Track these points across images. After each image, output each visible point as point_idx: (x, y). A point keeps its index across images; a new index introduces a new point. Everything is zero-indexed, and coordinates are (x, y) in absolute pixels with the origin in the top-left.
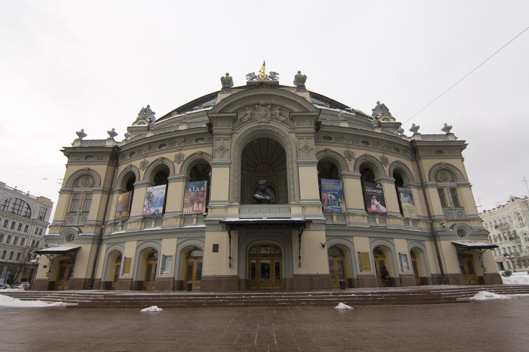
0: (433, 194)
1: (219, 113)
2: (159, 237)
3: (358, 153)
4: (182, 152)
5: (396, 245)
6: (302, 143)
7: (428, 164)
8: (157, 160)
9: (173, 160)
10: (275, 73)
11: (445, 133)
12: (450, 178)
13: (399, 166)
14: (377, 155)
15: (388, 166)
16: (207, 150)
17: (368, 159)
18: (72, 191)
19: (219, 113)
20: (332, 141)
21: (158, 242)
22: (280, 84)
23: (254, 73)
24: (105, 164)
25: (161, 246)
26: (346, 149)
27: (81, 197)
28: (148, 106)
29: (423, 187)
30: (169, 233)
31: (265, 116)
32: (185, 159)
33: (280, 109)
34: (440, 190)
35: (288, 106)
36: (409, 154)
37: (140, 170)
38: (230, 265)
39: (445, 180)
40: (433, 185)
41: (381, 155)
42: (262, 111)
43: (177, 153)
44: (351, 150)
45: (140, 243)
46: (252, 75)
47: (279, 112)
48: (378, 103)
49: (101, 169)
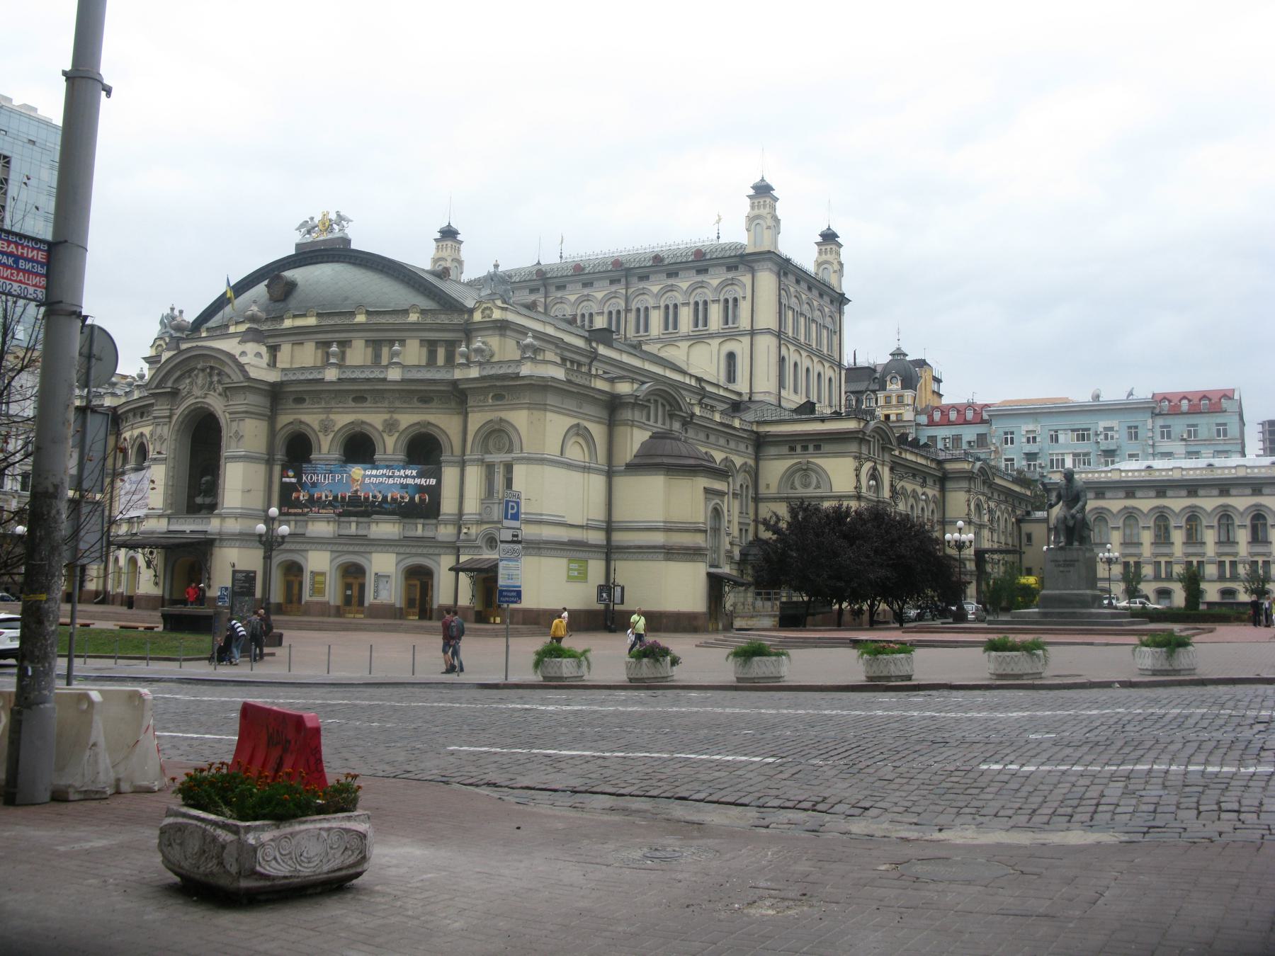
0: (474, 475)
1: (157, 387)
3: (343, 419)
5: (373, 561)
7: (477, 420)
13: (423, 430)
15: (397, 435)
17: (358, 429)
19: (157, 387)
20: (305, 406)
26: (323, 416)
29: (462, 464)
31: (202, 388)
33: (219, 374)
34: (490, 468)
36: (453, 405)
38: (156, 584)
39: (499, 450)
40: (474, 461)
41: (387, 416)
44: (332, 416)
48: (496, 266)
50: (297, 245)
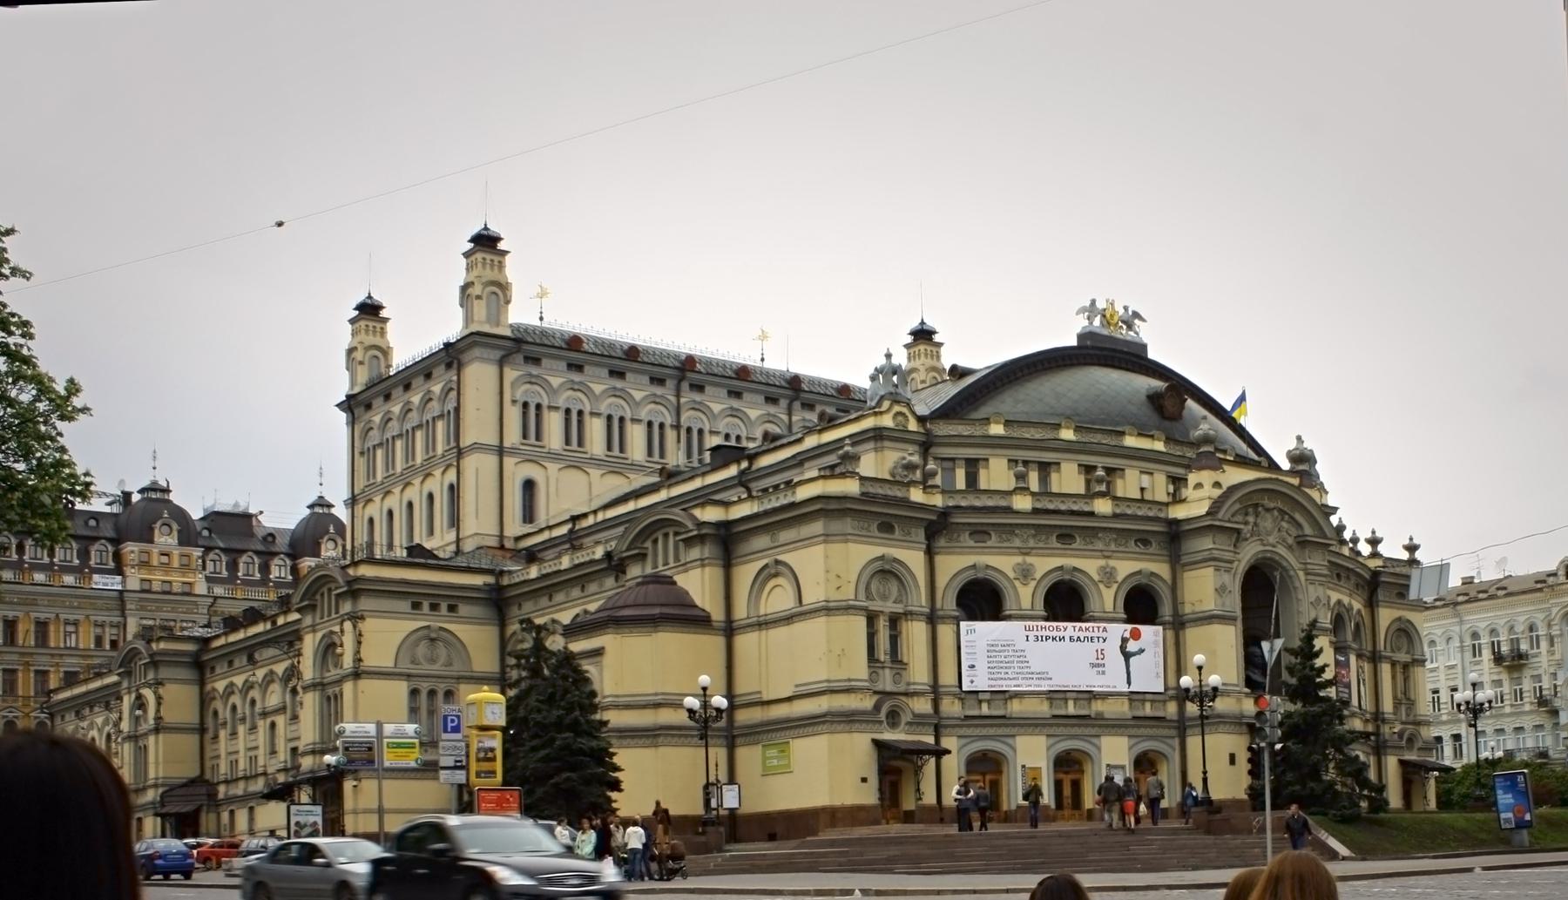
2: (1094, 731)
4: (1112, 563)
6: (1314, 592)
7: (1386, 616)
8: (1061, 568)
9: (1096, 578)
10: (1136, 315)
11: (1405, 556)
12: (1405, 649)
14: (1346, 600)
16: (1162, 569)
18: (865, 609)
21: (1095, 740)
22: (1152, 354)
23: (1093, 302)
24: (919, 549)
25: (1099, 749)
27: (882, 625)
28: (889, 356)
30: (1114, 726)
32: (1120, 578)
35: (1298, 516)
37: (1017, 583)
42: (1267, 522)
43: (1102, 562)
45: (1052, 740)
46: (1091, 310)
47: (1284, 524)
49: (914, 559)
50: (1081, 337)
